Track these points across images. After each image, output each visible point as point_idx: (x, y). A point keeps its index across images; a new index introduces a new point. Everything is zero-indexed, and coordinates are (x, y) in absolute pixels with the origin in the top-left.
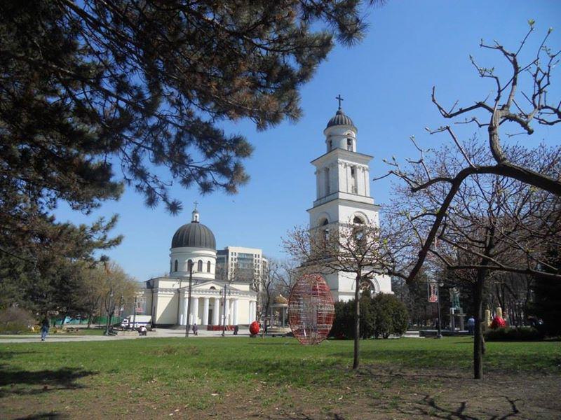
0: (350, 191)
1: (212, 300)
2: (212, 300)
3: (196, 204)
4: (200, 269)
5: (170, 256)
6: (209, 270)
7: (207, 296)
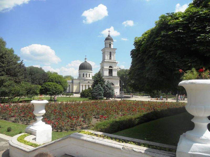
0: (109, 59)
5: (79, 72)
6: (89, 76)
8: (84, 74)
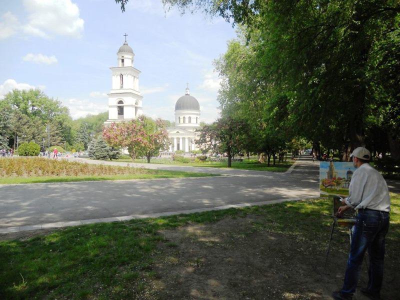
1: (178, 139)
2: (178, 139)
3: (187, 84)
4: (184, 122)
6: (190, 122)
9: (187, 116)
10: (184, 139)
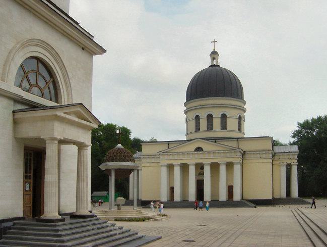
1: (200, 167)
2: (200, 167)
3: (214, 42)
7: (192, 161)
8: (197, 118)
9: (217, 114)
10: (215, 167)
